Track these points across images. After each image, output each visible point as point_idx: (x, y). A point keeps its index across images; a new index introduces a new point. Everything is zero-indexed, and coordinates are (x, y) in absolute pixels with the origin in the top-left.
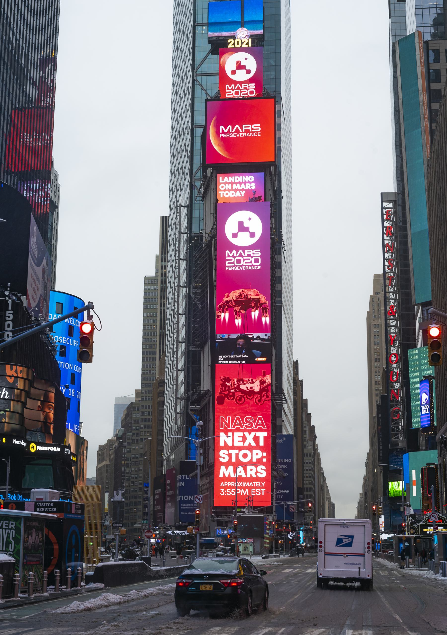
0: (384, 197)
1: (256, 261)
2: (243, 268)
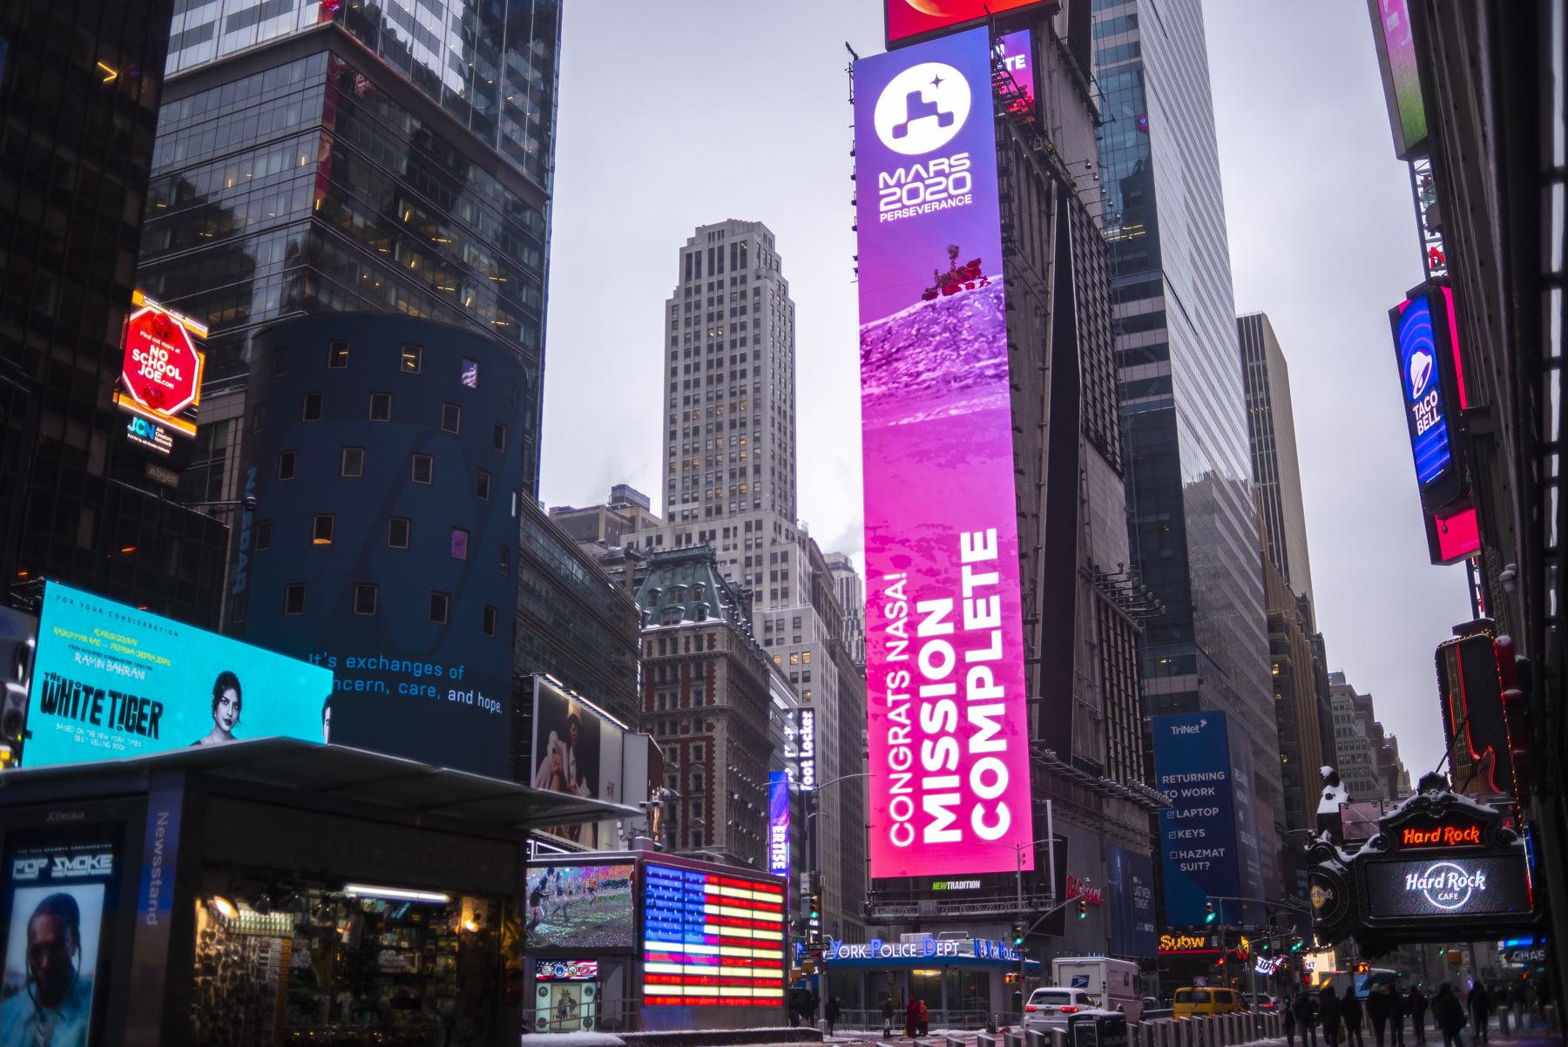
1: (959, 183)
2: (927, 209)
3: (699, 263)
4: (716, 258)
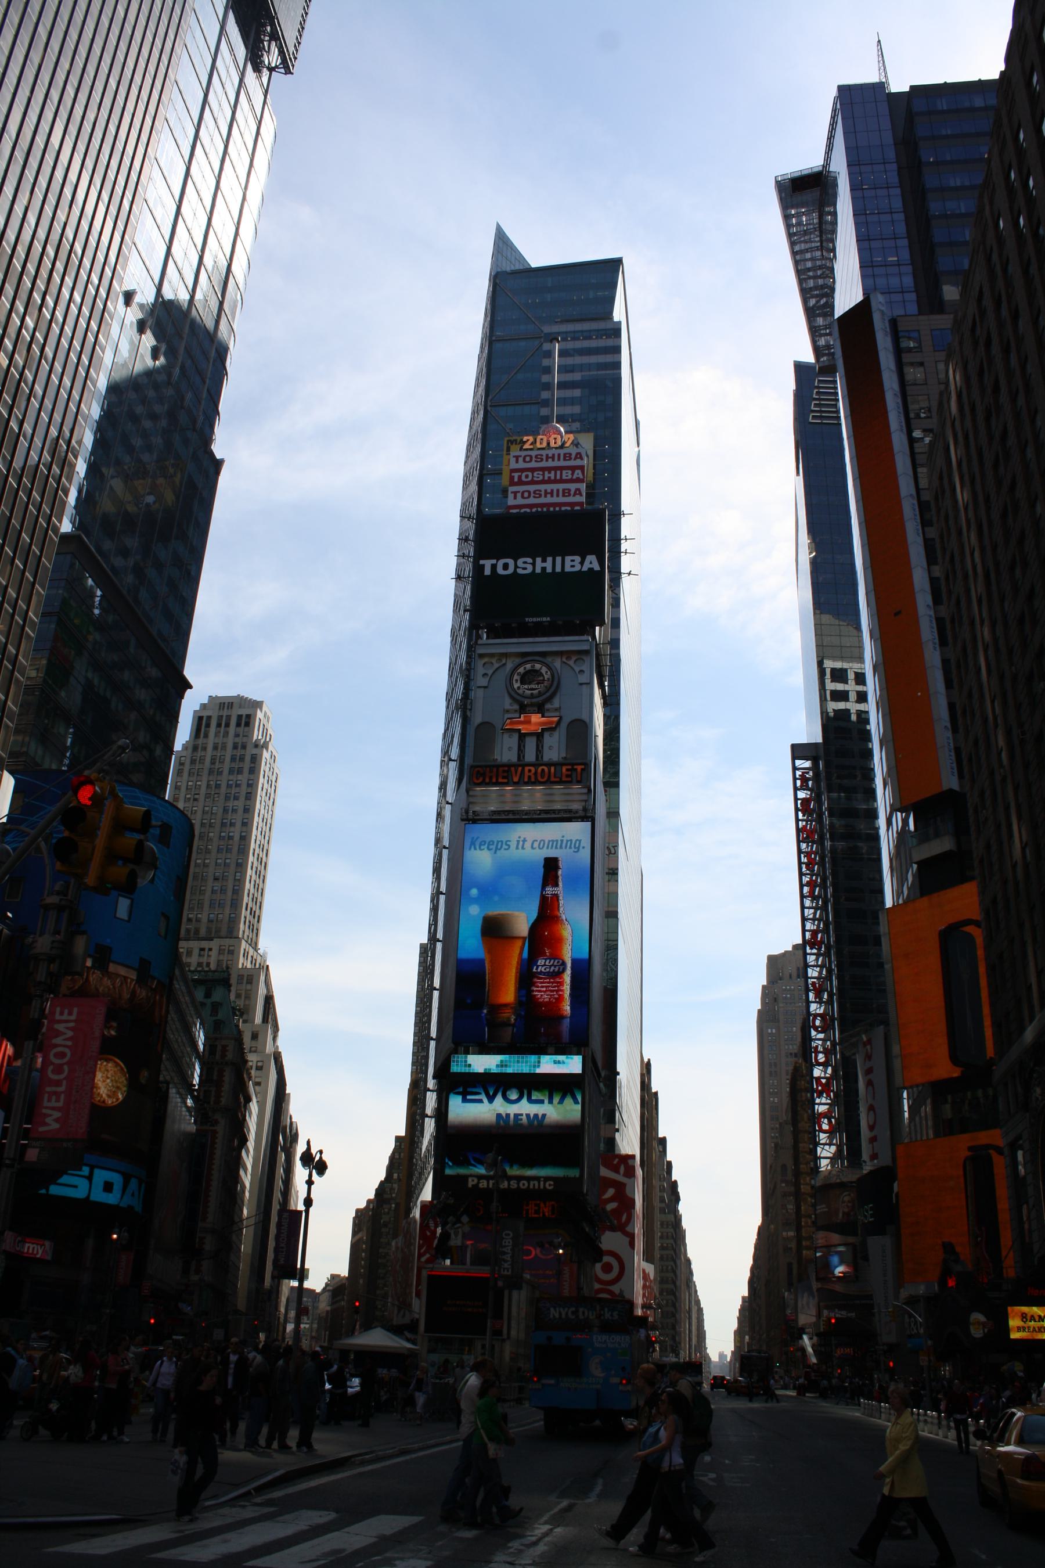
0: (798, 751)
3: (208, 725)
4: (223, 723)
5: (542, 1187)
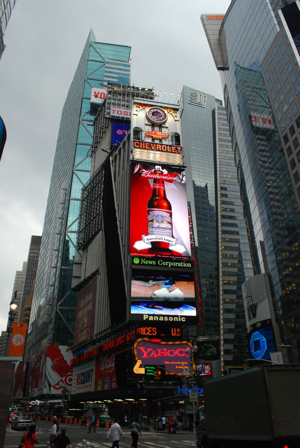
5: (180, 320)
